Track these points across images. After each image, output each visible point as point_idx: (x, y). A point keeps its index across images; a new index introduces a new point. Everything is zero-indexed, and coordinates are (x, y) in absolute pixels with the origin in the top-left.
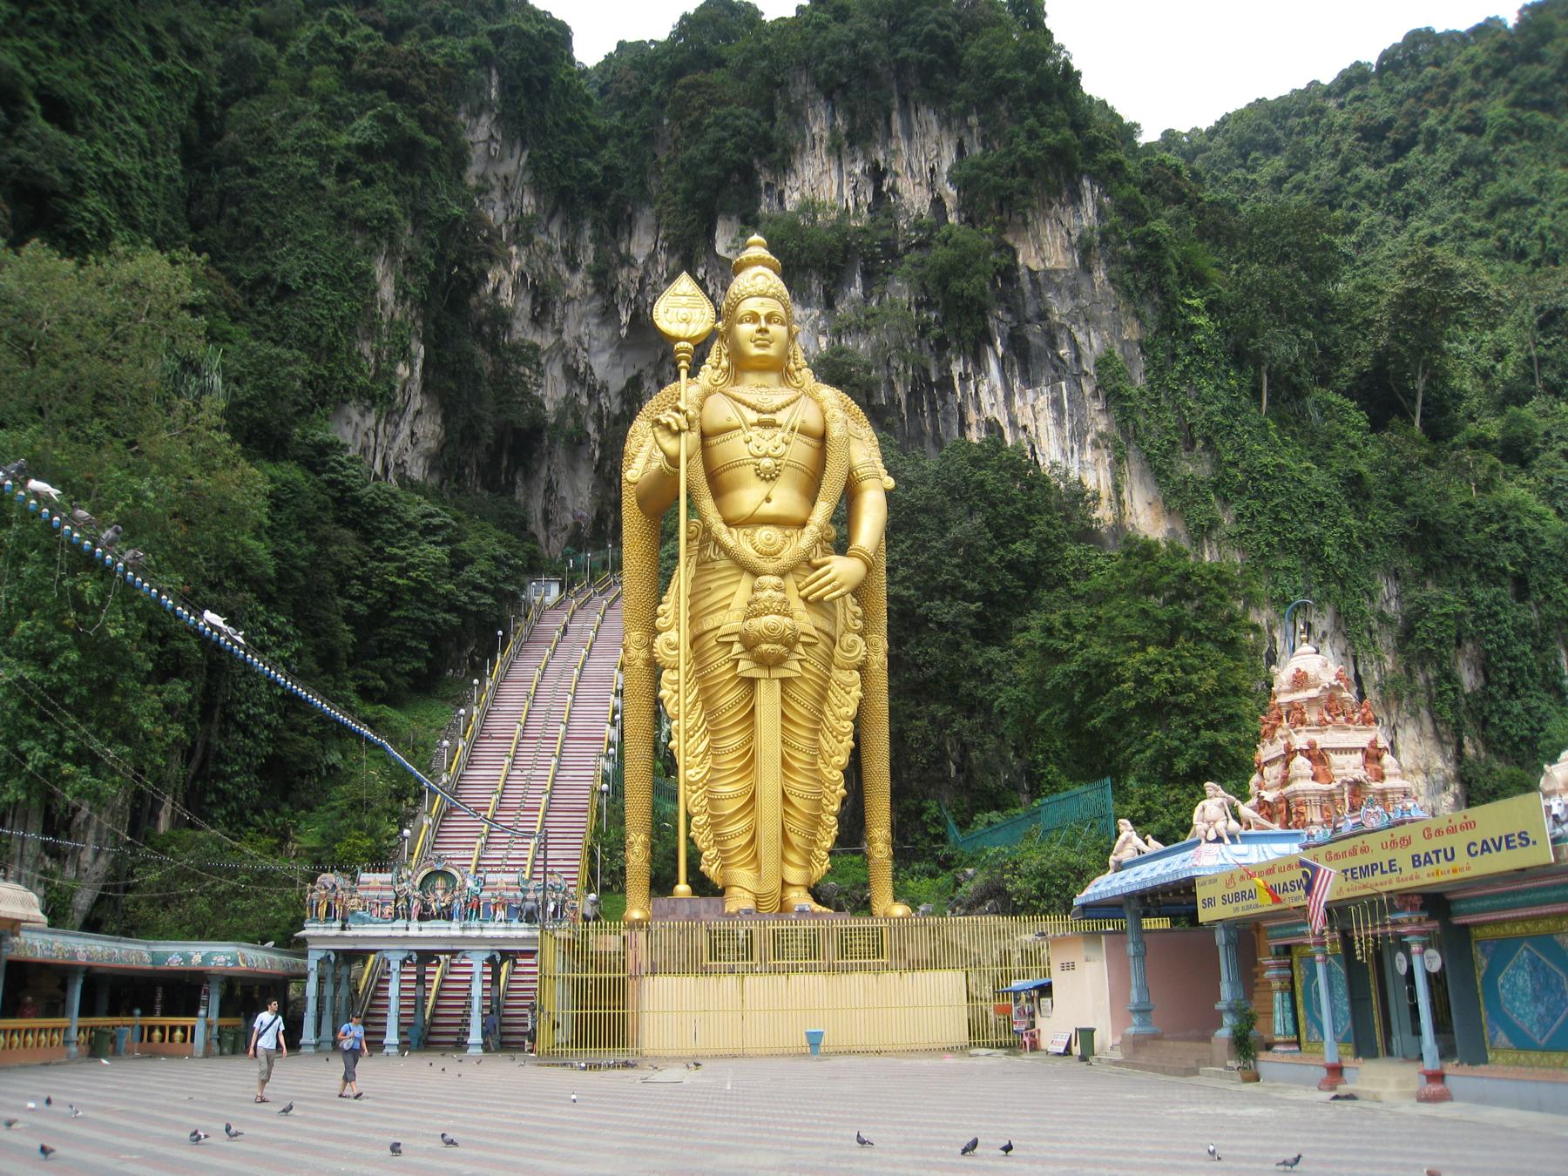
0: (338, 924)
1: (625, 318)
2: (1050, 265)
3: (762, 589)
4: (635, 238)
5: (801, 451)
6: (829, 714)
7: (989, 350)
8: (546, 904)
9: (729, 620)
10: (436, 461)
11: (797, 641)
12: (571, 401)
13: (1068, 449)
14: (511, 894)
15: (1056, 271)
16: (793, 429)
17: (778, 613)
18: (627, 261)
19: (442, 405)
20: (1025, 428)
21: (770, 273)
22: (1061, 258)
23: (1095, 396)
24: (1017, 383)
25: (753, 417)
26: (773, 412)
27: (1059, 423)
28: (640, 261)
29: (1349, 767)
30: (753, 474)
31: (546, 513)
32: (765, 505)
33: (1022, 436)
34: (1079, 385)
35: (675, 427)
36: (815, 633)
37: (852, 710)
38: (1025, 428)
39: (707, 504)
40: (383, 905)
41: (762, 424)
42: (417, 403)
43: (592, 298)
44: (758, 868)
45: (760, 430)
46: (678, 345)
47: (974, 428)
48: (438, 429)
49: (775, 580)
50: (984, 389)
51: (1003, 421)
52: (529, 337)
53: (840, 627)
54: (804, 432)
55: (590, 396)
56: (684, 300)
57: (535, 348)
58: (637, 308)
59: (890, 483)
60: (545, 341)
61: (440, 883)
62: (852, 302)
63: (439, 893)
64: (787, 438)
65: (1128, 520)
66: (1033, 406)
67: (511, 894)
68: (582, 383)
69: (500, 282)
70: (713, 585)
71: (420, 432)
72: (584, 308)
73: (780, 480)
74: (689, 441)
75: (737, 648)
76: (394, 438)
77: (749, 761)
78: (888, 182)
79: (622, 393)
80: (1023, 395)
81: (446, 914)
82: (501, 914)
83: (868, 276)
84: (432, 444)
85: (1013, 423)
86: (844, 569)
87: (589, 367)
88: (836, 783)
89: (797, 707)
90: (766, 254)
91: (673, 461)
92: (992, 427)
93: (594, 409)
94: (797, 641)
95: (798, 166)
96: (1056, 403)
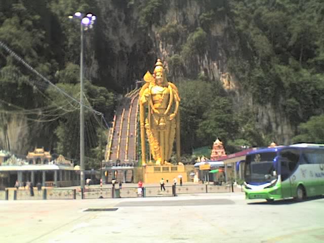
1: (132, 32)
18: (132, 18)
50: (204, 62)
51: (208, 68)
79: (132, 48)
81: (120, 165)
85: (209, 69)
96: (218, 65)
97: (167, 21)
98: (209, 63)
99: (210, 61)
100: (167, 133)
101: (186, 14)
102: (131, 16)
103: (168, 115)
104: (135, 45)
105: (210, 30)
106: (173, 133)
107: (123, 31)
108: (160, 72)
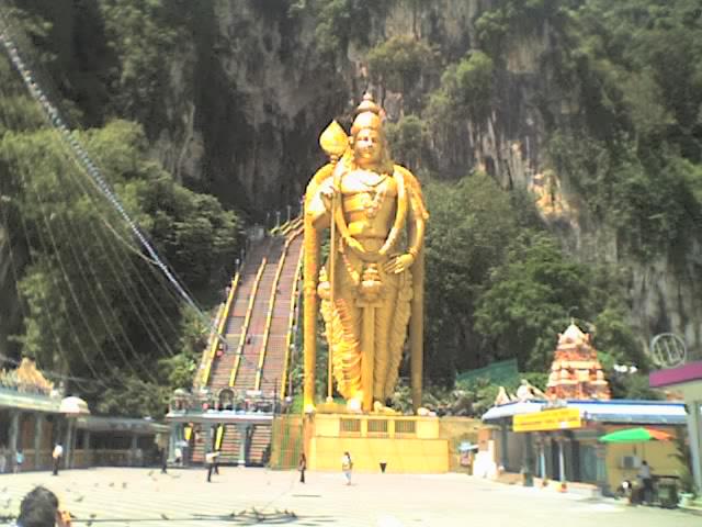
1: (297, 78)
4: (303, 34)
18: (298, 46)
29: (583, 376)
31: (254, 186)
33: (504, 165)
37: (406, 321)
38: (506, 161)
42: (190, 136)
51: (495, 157)
53: (402, 282)
78: (439, 22)
79: (295, 119)
81: (230, 408)
85: (499, 159)
87: (277, 104)
93: (280, 126)
95: (392, 12)
96: (522, 148)
97: (387, 35)
98: (498, 144)
99: (502, 137)
100: (385, 314)
101: (440, 16)
102: (296, 39)
103: (390, 257)
104: (302, 114)
105: (504, 56)
106: (403, 317)
107: (274, 75)
108: (372, 128)
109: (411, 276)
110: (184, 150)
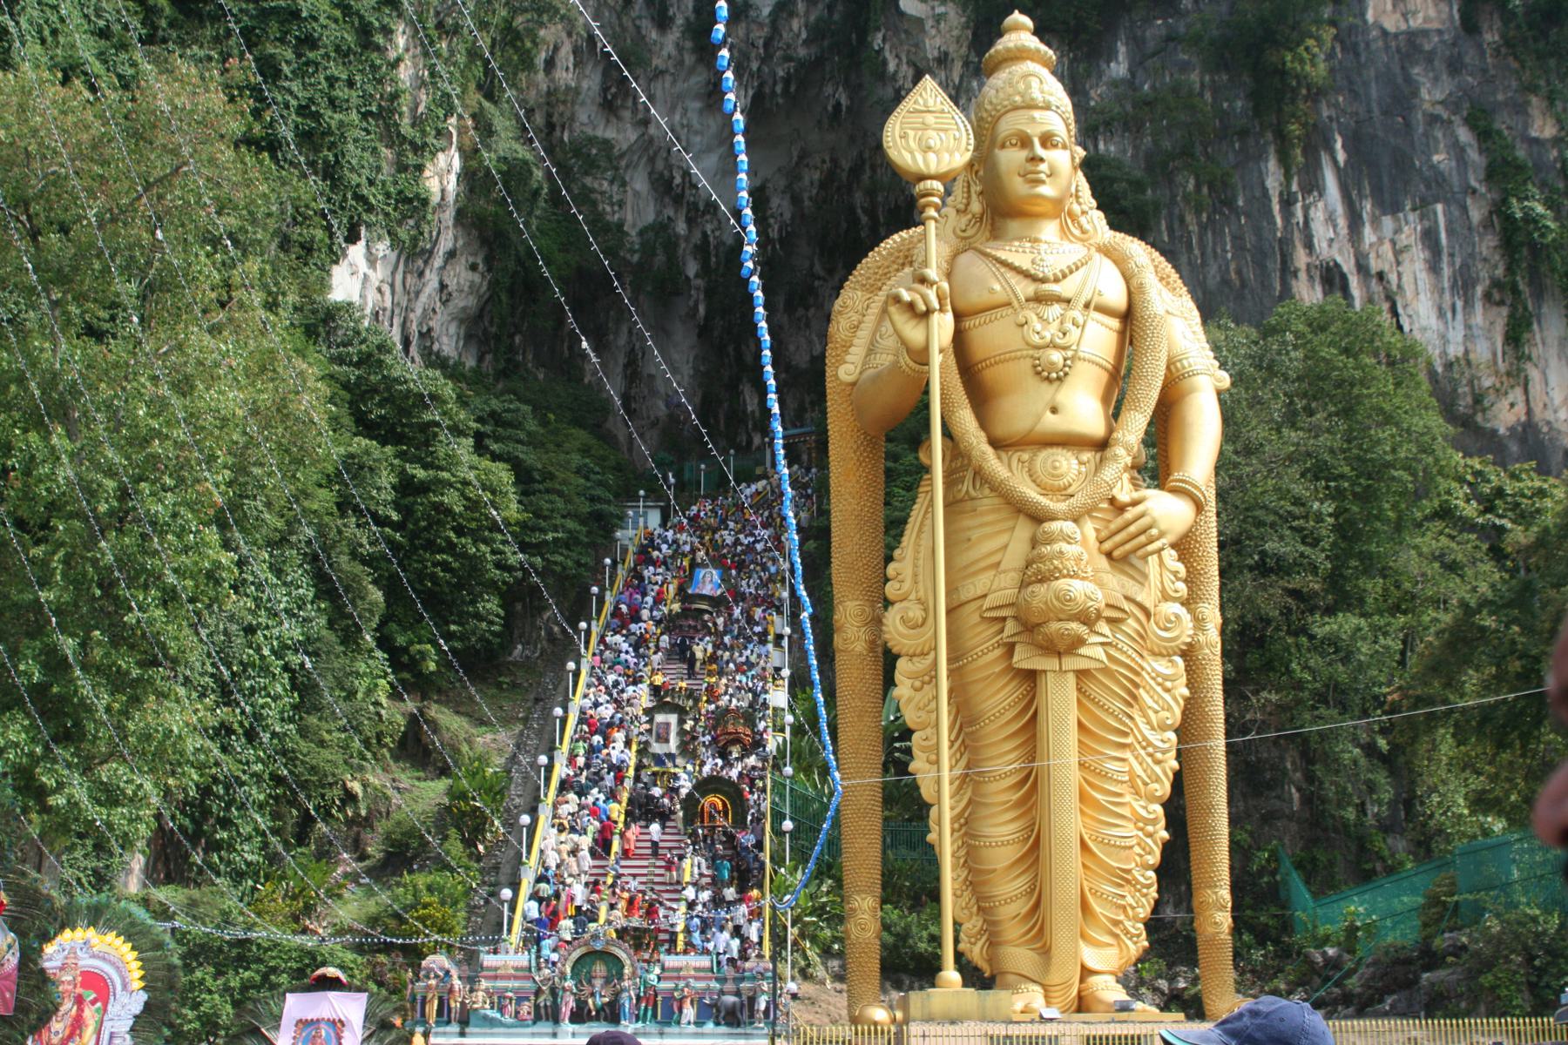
0: (455, 1028)
2: (1416, 23)
3: (1050, 540)
5: (1100, 338)
6: (1139, 720)
7: (1325, 159)
8: (752, 1000)
9: (999, 587)
10: (475, 328)
11: (1099, 616)
12: (661, 228)
13: (1447, 305)
14: (701, 985)
15: (1425, 33)
16: (1087, 306)
17: (1075, 576)
19: (484, 241)
20: (1381, 276)
21: (1045, 73)
22: (1432, 12)
23: (1487, 224)
24: (1368, 206)
25: (1024, 289)
26: (1057, 280)
27: (1434, 268)
28: (766, 11)
30: (1030, 371)
32: (1048, 413)
33: (1375, 285)
34: (1464, 209)
35: (924, 308)
36: (1126, 606)
38: (1381, 276)
39: (966, 419)
40: (520, 1000)
41: (1040, 299)
43: (692, 71)
44: (1045, 952)
45: (1041, 309)
46: (922, 186)
47: (1302, 275)
48: (477, 278)
49: (1068, 527)
50: (1318, 215)
52: (599, 133)
54: (1101, 309)
55: (690, 221)
56: (930, 119)
57: (607, 145)
58: (761, 85)
59: (1225, 380)
60: (623, 135)
61: (600, 969)
62: (1115, 84)
63: (598, 983)
64: (1080, 320)
65: (1539, 414)
66: (1393, 243)
67: (701, 985)
68: (678, 200)
69: (556, 49)
70: (975, 535)
71: (452, 284)
72: (681, 86)
73: (1069, 378)
74: (943, 327)
75: (1011, 627)
76: (418, 294)
77: (1031, 788)
80: (1376, 223)
82: (689, 1012)
83: (1136, 43)
84: (471, 302)
85: (1362, 268)
86: (1167, 511)
88: (1154, 822)
89: (1098, 712)
90: (1033, 42)
91: (921, 356)
92: (1332, 278)
93: (697, 237)
94: (1099, 616)
96: (1429, 238)
109: (1181, 568)
110: (432, 279)
